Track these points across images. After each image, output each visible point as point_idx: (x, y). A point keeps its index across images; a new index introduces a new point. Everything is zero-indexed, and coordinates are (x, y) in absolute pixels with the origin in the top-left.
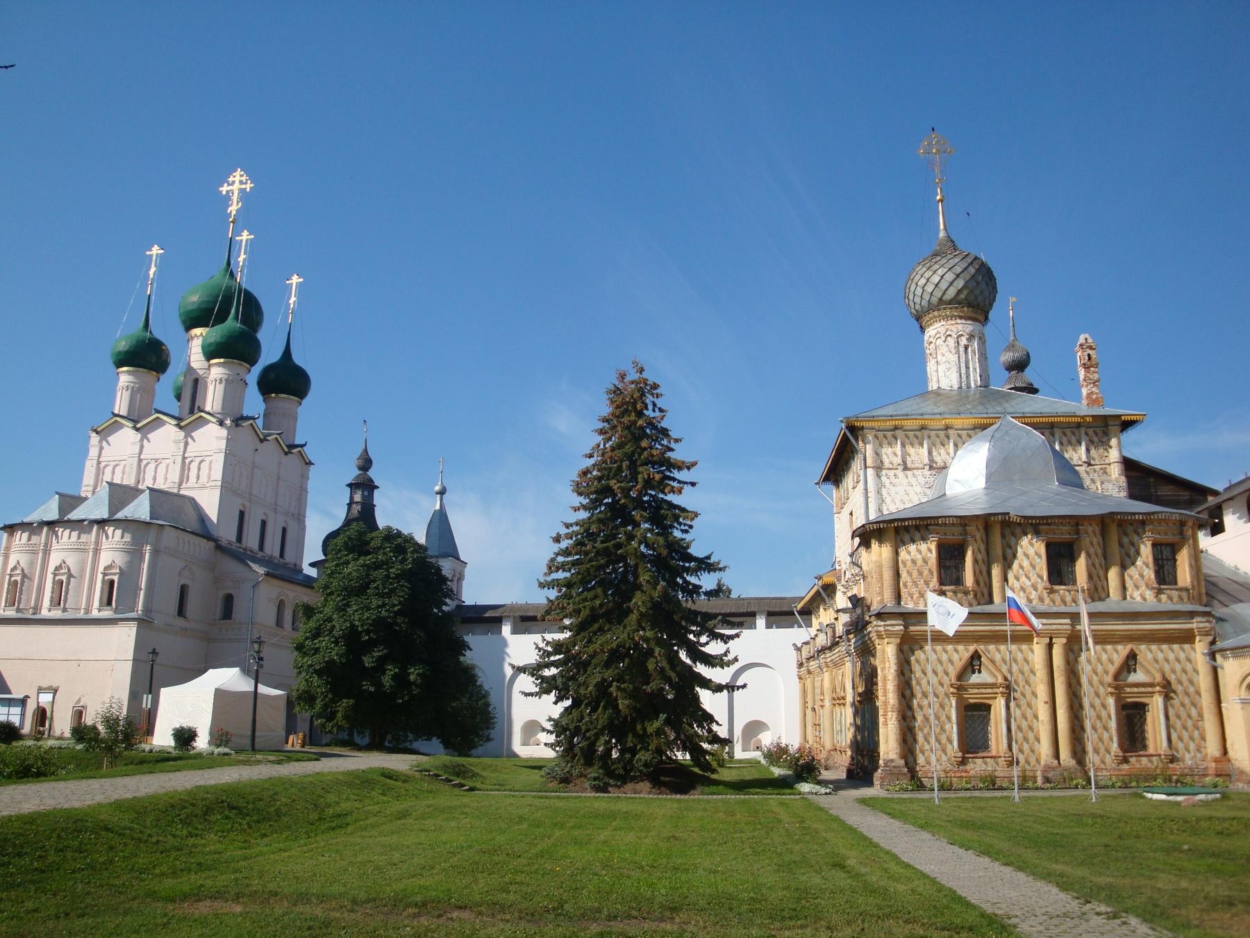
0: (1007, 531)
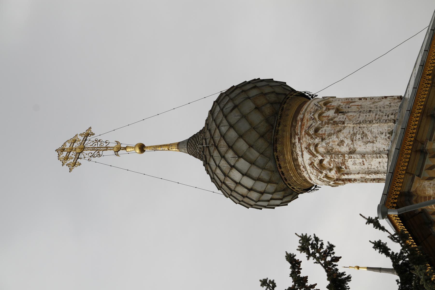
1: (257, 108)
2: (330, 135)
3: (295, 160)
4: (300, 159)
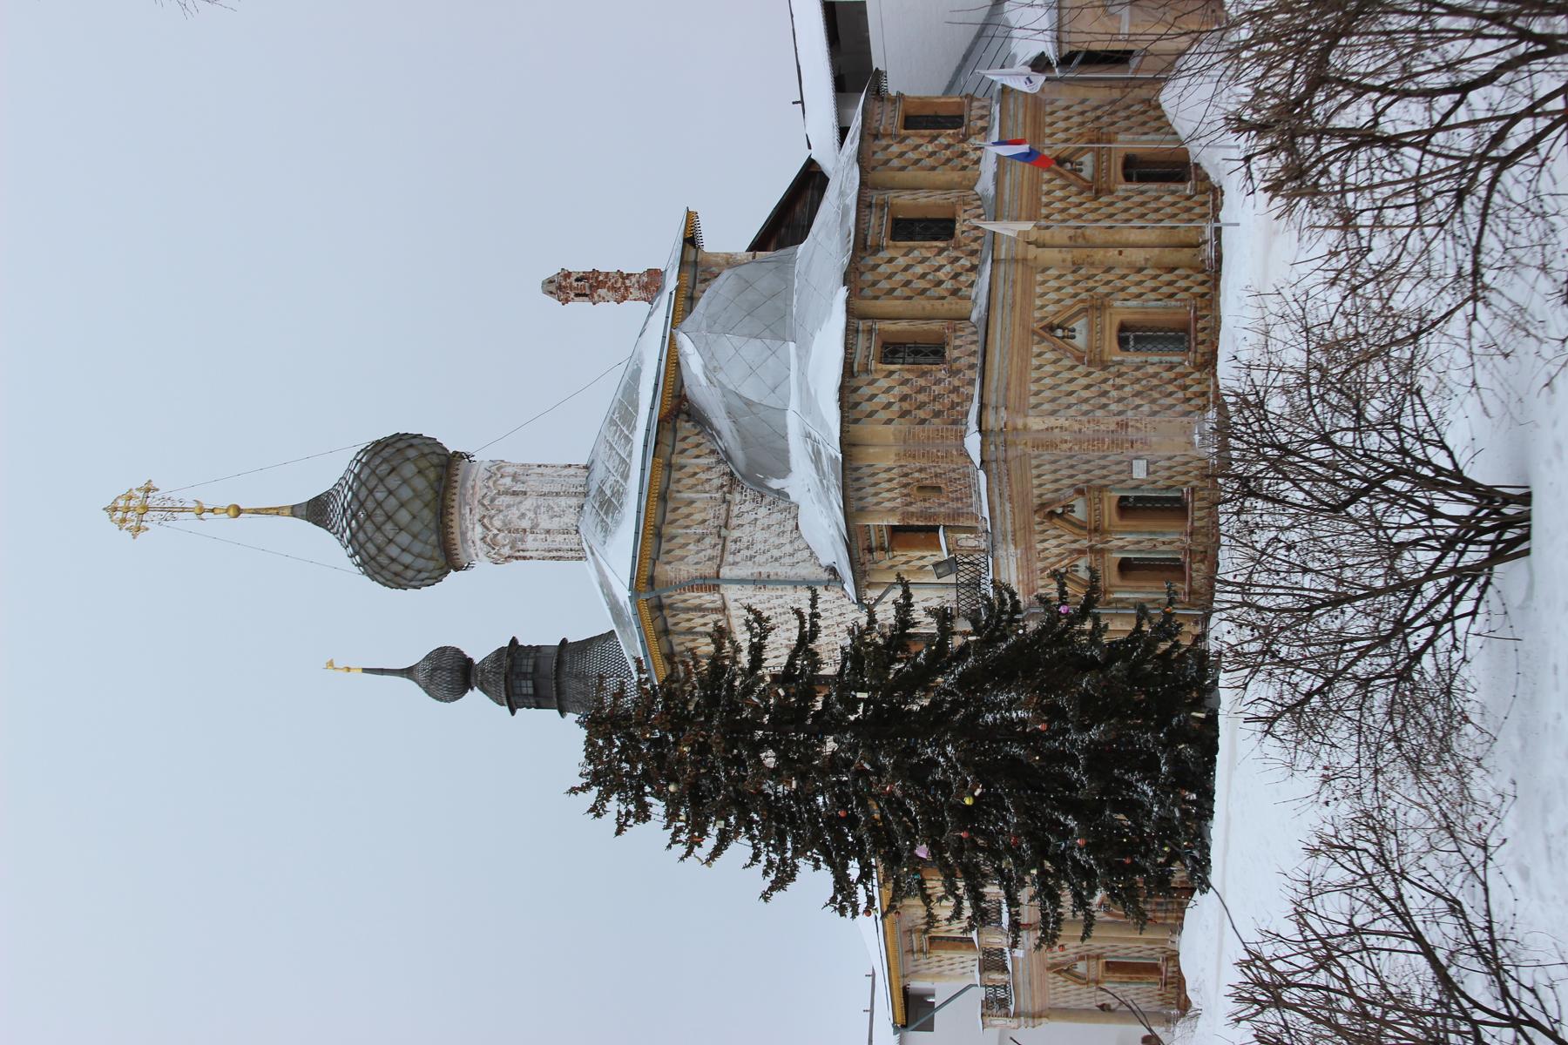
0: (868, 292)
1: (420, 472)
2: (508, 506)
3: (463, 534)
4: (469, 534)
